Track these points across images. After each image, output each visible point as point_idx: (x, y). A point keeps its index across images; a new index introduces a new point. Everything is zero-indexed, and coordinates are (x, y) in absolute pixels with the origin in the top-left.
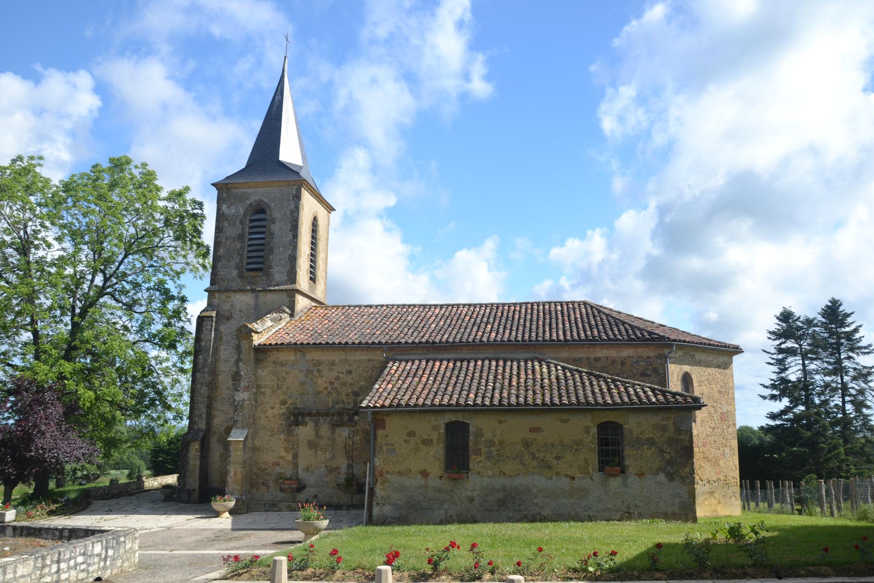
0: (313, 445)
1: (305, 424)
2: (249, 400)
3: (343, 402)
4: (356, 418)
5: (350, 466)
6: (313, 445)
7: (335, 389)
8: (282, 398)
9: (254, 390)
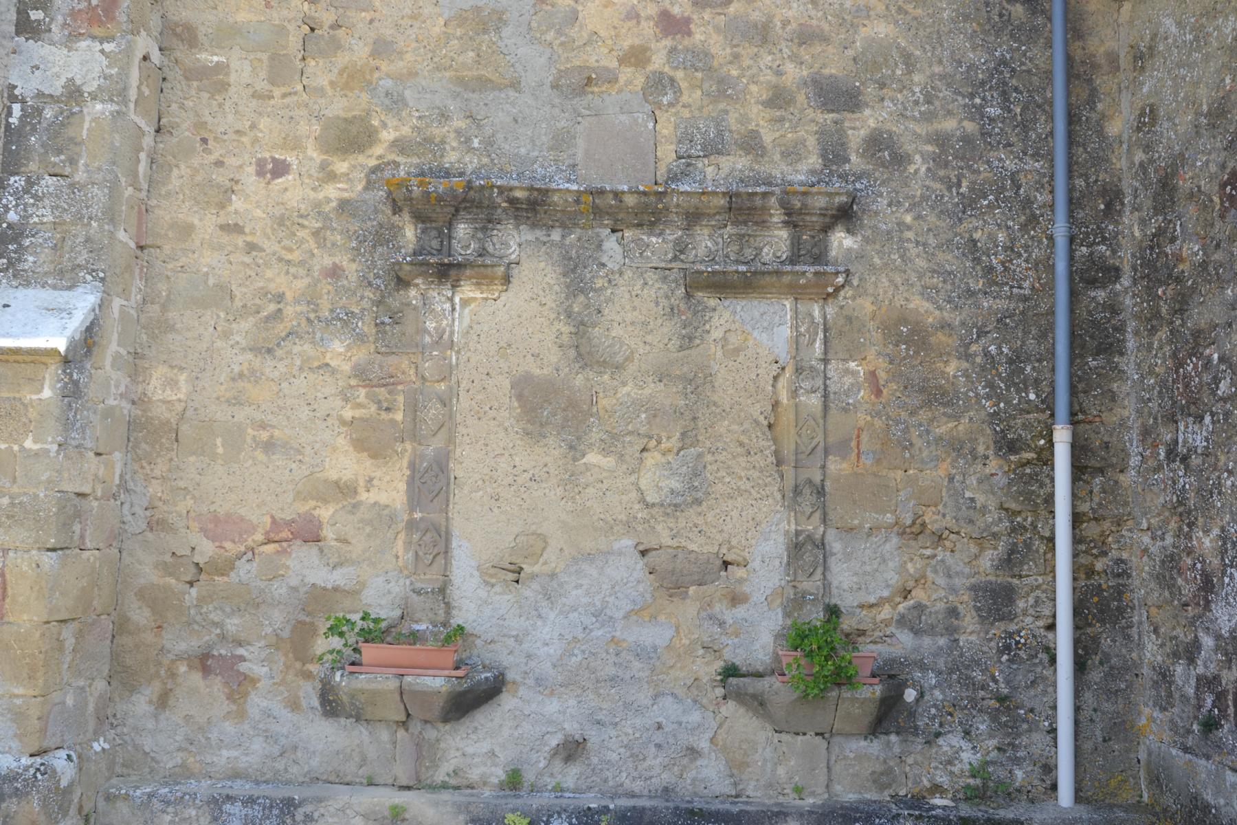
0: (547, 409)
1: (494, 272)
2: (115, 91)
3: (751, 144)
4: (842, 241)
5: (805, 551)
6: (547, 409)
7: (699, 60)
8: (337, 107)
9: (144, 43)
